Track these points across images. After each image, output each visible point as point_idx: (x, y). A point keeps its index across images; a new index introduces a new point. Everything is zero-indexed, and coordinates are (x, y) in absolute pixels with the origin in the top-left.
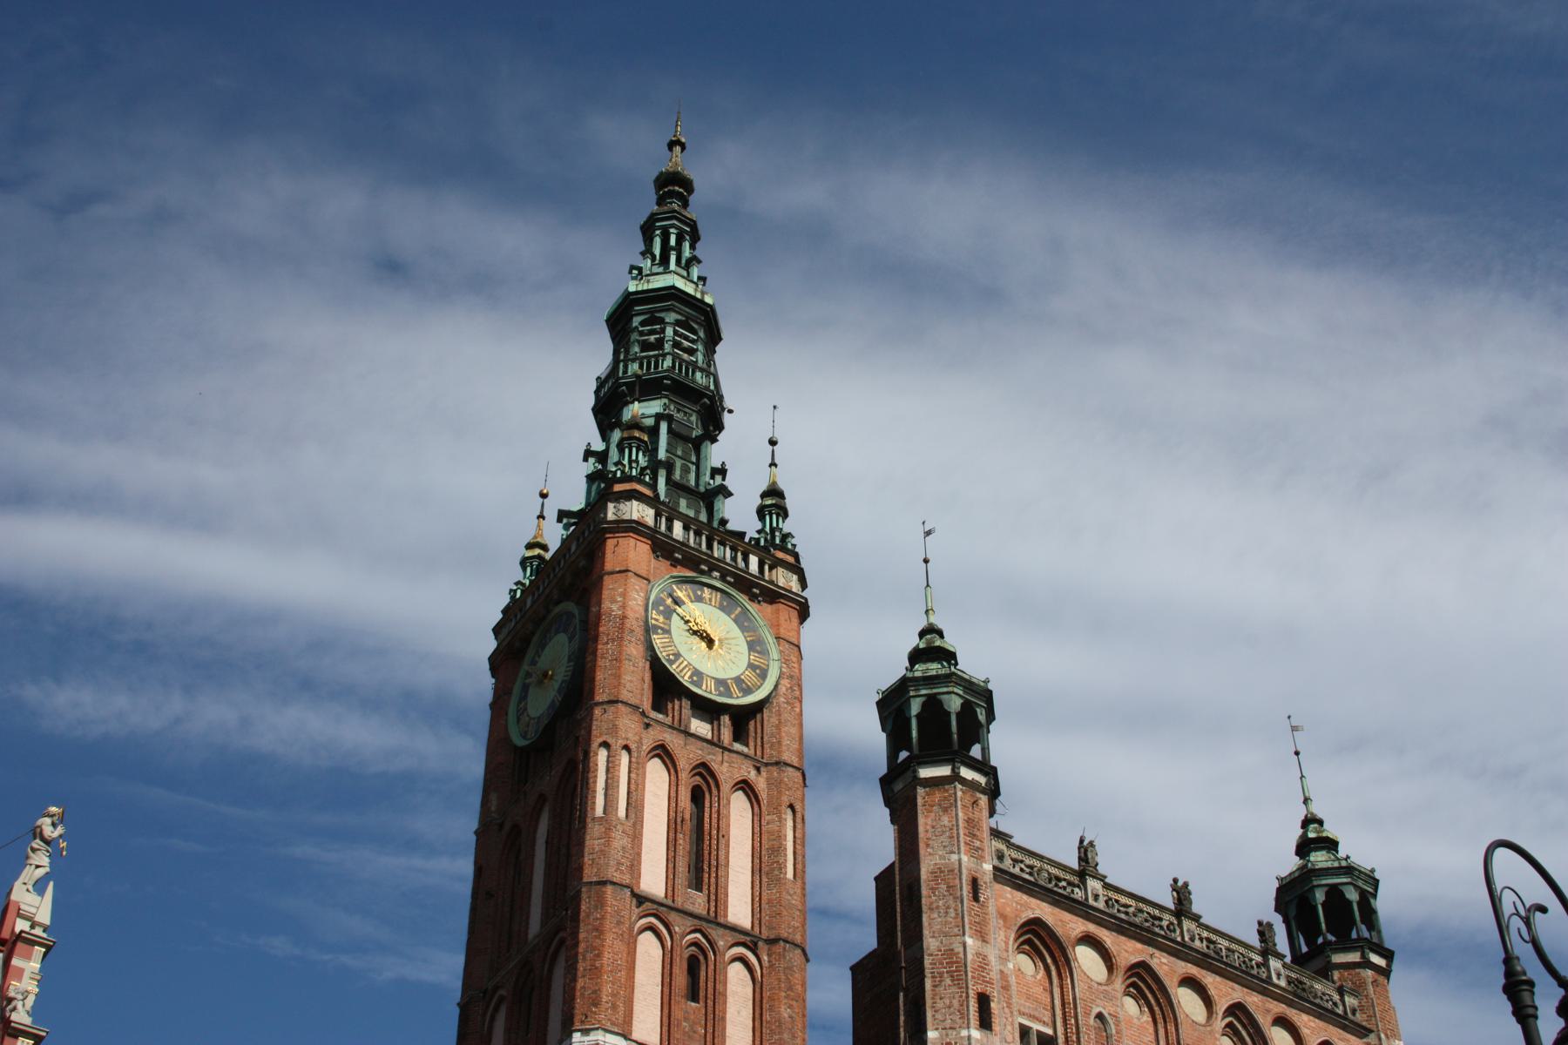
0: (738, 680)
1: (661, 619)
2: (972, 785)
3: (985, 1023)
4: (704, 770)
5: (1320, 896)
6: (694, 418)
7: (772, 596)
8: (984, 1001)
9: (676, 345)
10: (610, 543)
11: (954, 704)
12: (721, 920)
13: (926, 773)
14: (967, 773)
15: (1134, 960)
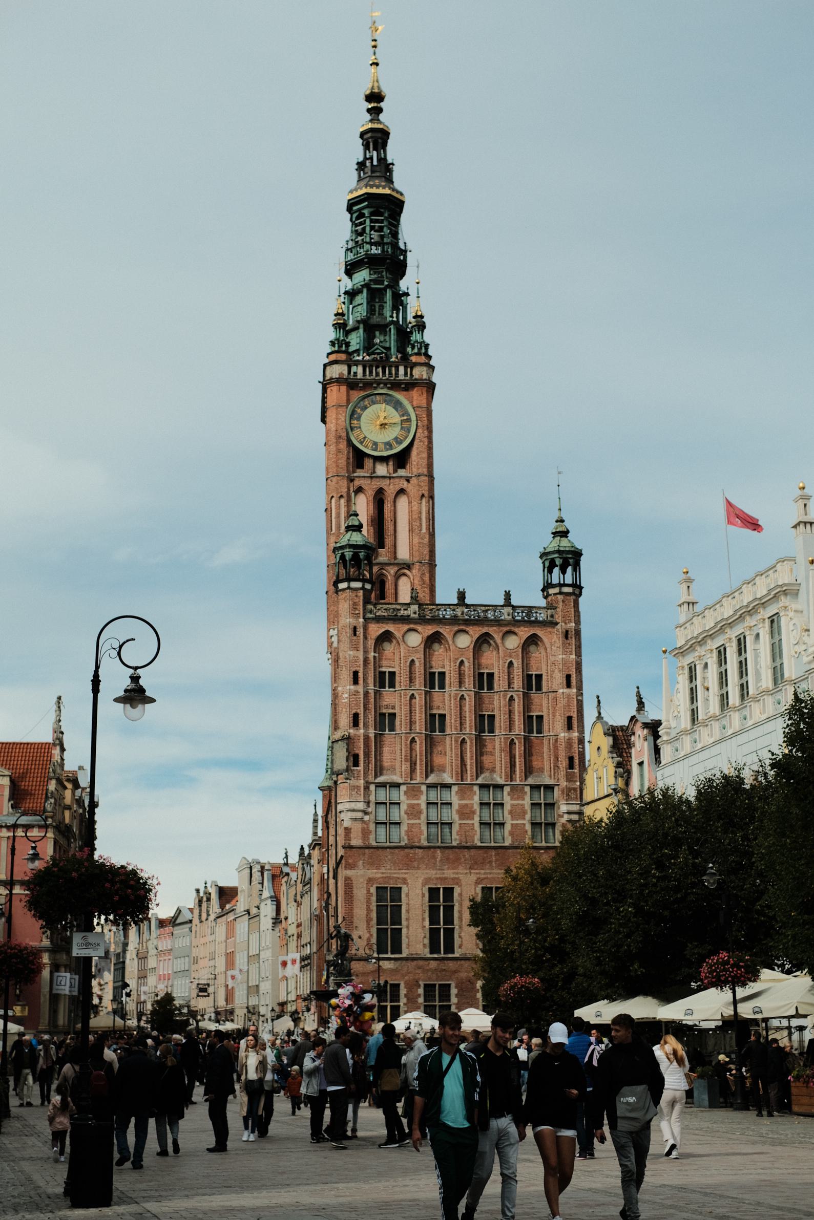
0: (396, 439)
1: (355, 422)
2: (356, 589)
3: (356, 682)
4: (380, 492)
5: (547, 564)
6: (384, 274)
7: (409, 386)
8: (356, 674)
9: (372, 228)
10: (329, 390)
11: (348, 554)
12: (392, 561)
13: (342, 586)
14: (354, 585)
15: (431, 632)
